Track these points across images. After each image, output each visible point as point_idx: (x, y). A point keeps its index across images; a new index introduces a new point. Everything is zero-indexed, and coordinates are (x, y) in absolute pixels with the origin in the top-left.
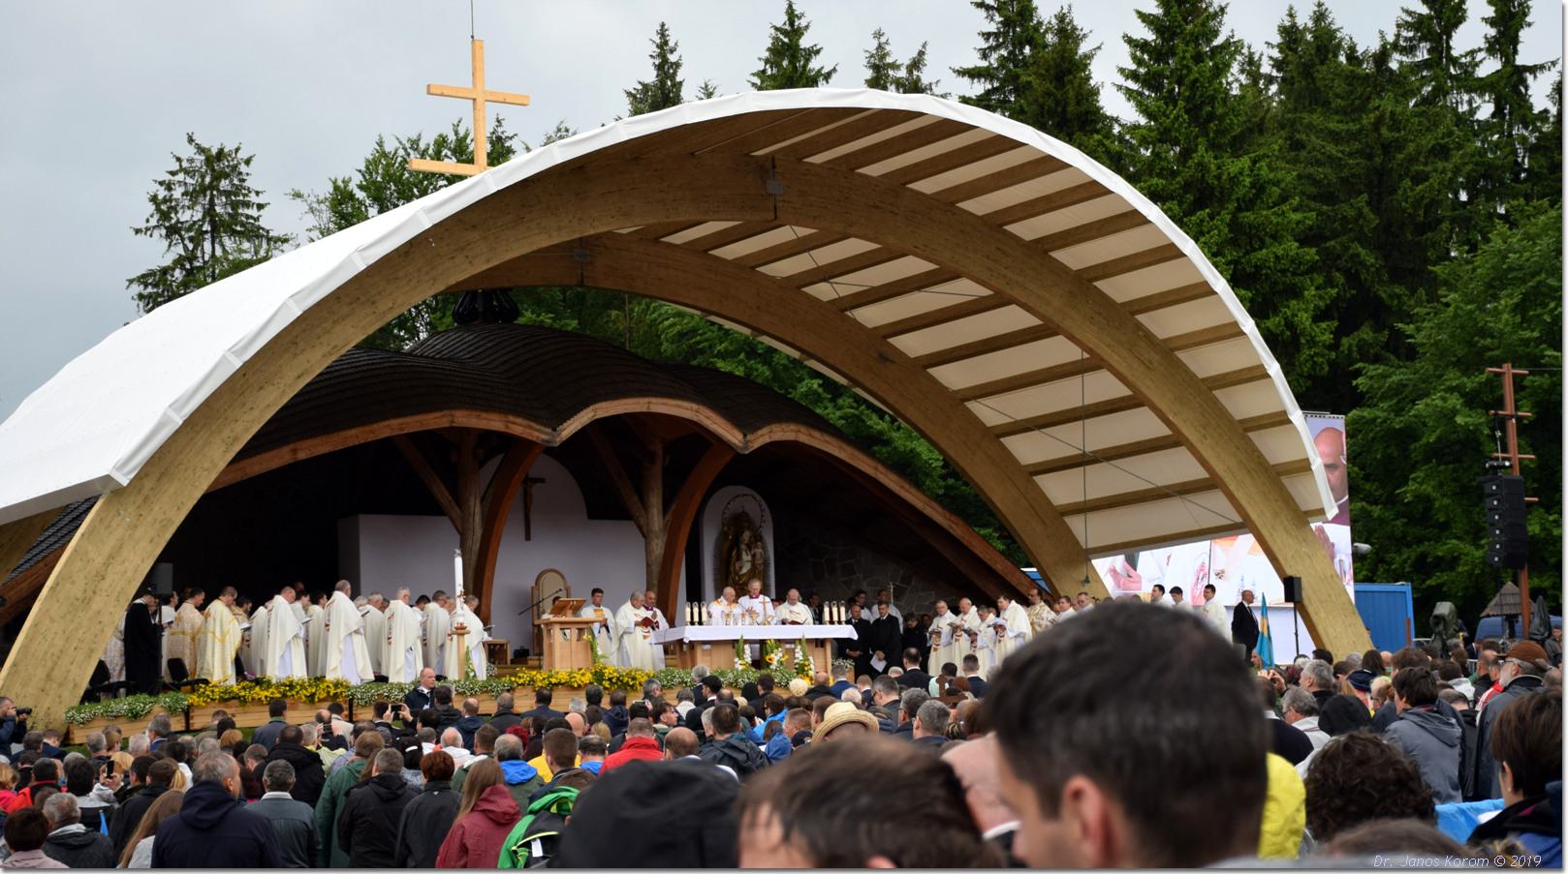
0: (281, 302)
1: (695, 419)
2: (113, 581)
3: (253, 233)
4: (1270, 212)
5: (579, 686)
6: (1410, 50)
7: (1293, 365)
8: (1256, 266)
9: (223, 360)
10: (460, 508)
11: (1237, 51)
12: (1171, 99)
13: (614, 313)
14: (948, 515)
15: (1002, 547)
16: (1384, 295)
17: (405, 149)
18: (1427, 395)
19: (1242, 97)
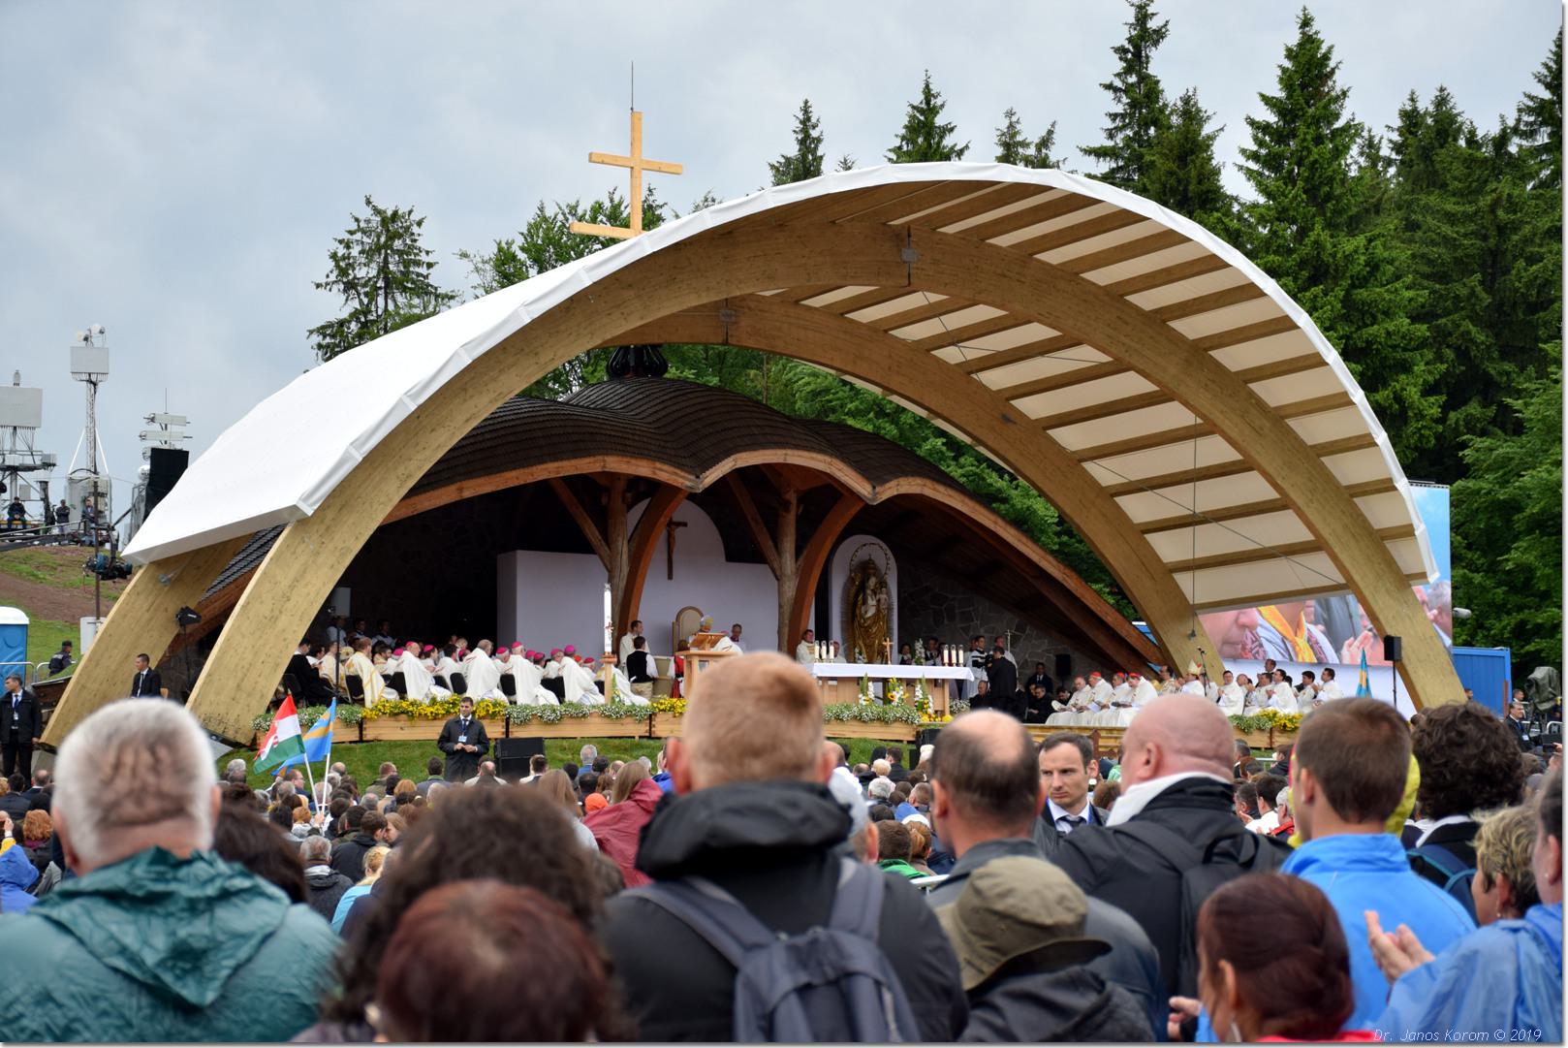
1: (828, 471)
3: (423, 289)
4: (1382, 290)
6: (1530, 134)
7: (1401, 437)
8: (1367, 342)
9: (400, 403)
10: (609, 547)
11: (1358, 134)
12: (1290, 179)
14: (1062, 567)
15: (1112, 601)
16: (1493, 372)
17: (564, 214)
18: (1534, 469)
19: (1361, 178)
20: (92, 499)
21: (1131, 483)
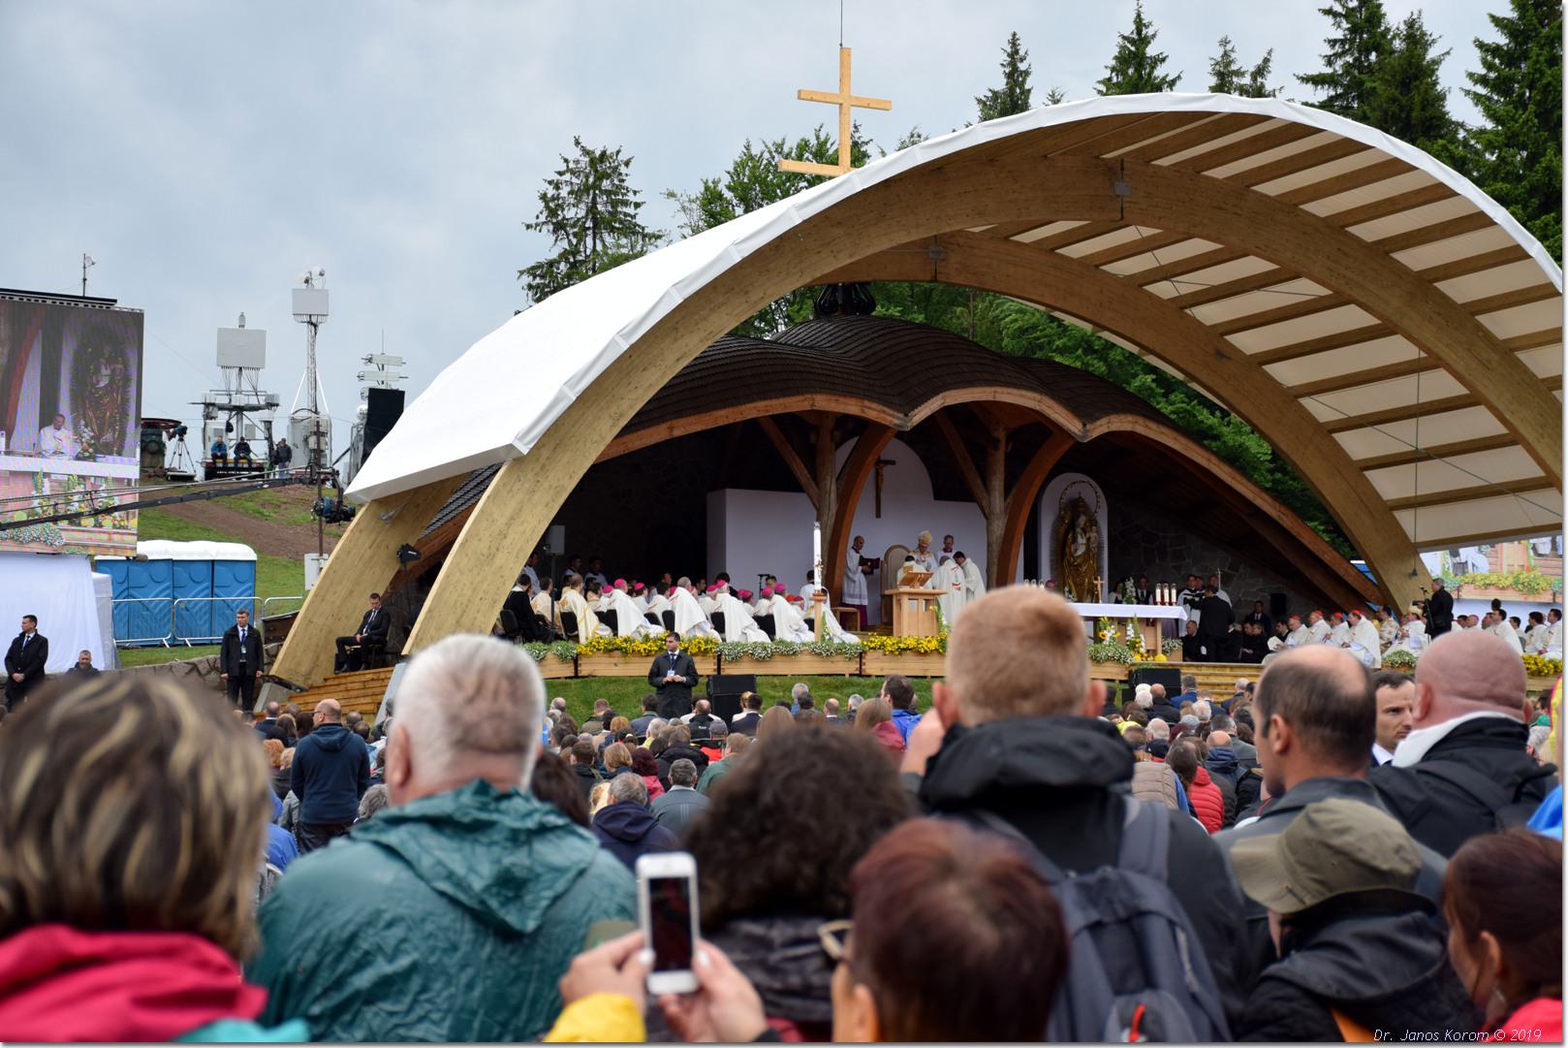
0: (665, 290)
1: (1038, 408)
2: (514, 539)
3: (630, 229)
5: (926, 651)
9: (612, 343)
10: (817, 484)
12: (1521, 103)
13: (959, 310)
14: (1277, 504)
15: (1327, 539)
17: (770, 152)
20: (312, 440)
21: (1350, 418)
